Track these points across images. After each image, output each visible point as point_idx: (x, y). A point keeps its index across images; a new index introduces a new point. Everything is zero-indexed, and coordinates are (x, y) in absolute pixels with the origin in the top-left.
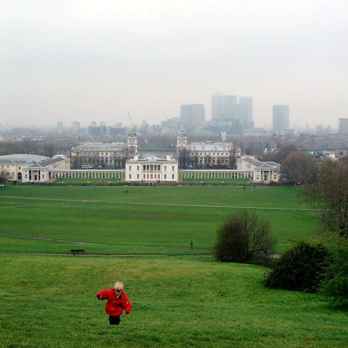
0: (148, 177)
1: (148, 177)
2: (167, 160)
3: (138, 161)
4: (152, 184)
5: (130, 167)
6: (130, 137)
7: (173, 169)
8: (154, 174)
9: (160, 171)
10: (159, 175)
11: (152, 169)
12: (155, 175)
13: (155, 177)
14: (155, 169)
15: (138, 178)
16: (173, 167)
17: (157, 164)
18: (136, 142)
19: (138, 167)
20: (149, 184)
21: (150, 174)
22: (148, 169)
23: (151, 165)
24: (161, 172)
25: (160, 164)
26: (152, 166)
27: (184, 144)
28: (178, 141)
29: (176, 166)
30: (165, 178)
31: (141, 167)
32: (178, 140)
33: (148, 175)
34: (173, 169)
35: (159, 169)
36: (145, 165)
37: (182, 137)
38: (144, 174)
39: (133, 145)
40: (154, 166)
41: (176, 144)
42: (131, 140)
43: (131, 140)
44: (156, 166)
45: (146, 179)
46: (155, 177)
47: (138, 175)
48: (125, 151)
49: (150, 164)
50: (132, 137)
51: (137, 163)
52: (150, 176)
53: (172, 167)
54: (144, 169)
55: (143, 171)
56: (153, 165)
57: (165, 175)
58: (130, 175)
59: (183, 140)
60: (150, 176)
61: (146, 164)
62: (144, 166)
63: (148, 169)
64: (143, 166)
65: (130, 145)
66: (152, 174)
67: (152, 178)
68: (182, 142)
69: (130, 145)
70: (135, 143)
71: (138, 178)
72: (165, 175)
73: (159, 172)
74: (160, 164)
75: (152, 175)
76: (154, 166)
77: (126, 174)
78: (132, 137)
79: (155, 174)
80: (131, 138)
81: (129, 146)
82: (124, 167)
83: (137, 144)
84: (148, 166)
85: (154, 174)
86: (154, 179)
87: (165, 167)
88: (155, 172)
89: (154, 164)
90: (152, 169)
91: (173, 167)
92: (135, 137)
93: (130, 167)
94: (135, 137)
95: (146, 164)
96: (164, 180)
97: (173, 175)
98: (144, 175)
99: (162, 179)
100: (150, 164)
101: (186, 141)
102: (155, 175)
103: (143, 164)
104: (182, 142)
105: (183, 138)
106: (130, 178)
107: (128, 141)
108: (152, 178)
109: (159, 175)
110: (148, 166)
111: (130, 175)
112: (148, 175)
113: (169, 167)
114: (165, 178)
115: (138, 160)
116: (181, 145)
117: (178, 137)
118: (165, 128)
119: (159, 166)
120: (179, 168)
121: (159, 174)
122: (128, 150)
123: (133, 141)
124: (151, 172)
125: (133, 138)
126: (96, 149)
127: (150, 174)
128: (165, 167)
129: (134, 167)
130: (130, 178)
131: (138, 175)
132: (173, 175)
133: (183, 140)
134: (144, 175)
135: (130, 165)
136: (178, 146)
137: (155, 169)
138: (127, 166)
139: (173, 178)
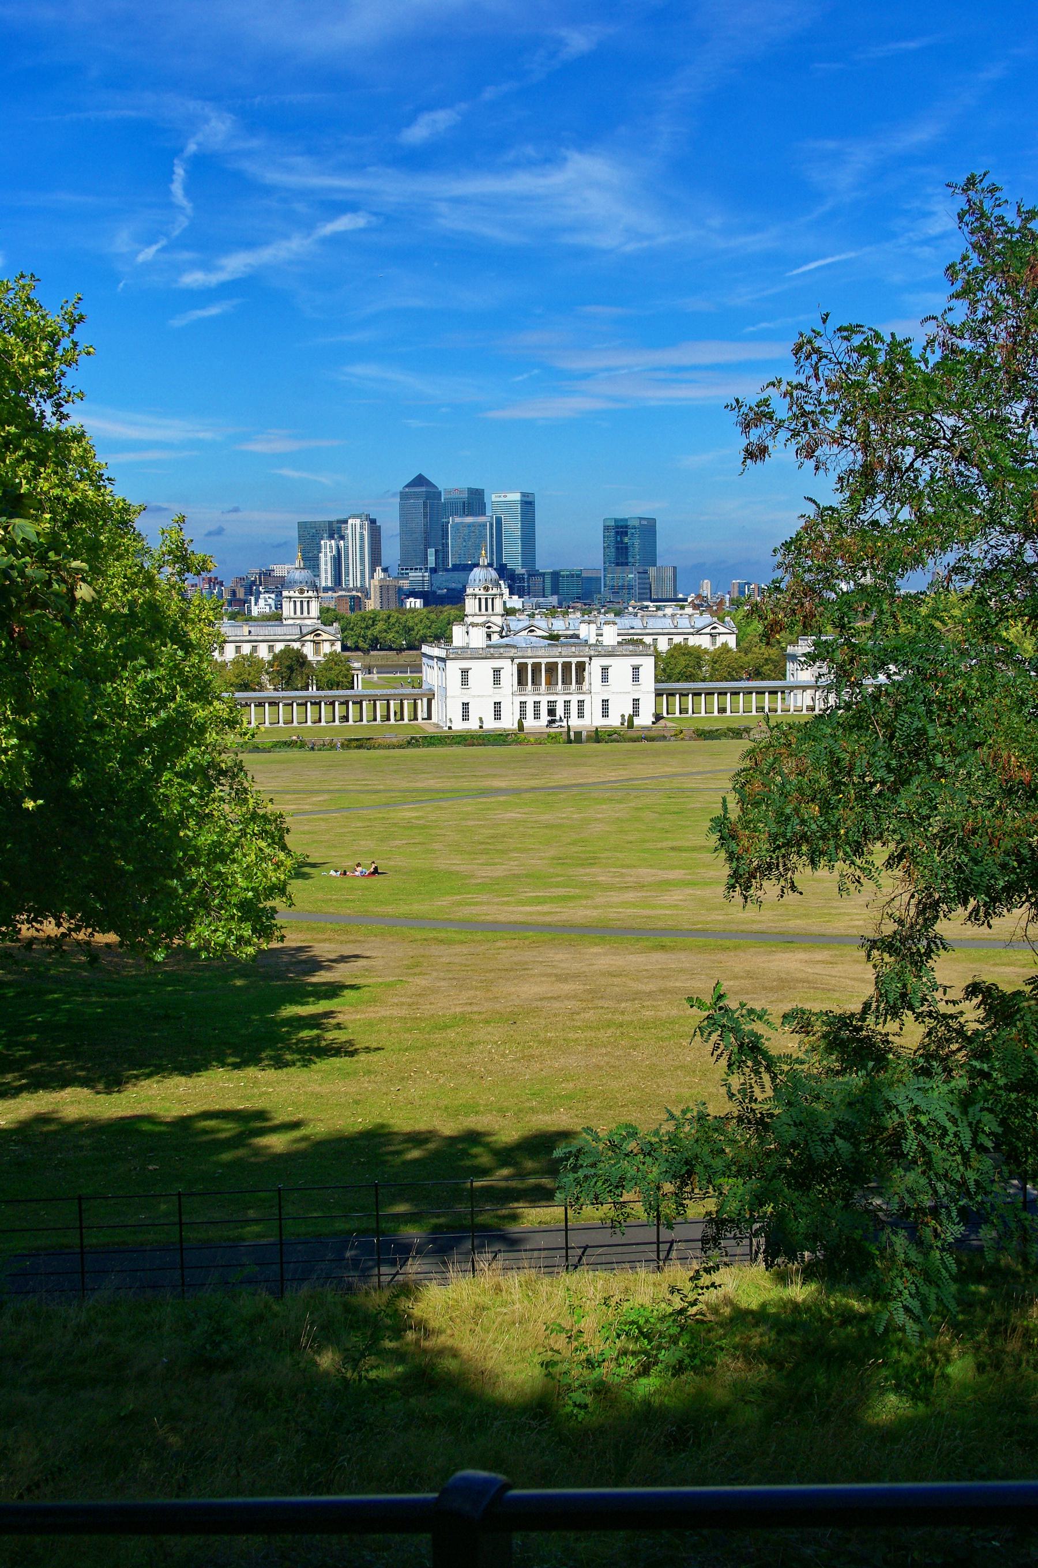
0: (537, 716)
1: (537, 716)
4: (584, 734)
5: (465, 672)
6: (292, 594)
7: (636, 678)
8: (560, 700)
9: (585, 686)
10: (581, 703)
11: (551, 682)
12: (567, 703)
15: (497, 716)
16: (636, 669)
17: (574, 660)
19: (497, 672)
23: (547, 664)
25: (587, 659)
26: (551, 668)
29: (648, 666)
30: (605, 714)
31: (509, 672)
33: (537, 704)
34: (636, 678)
37: (487, 589)
38: (523, 699)
42: (298, 604)
43: (298, 604)
44: (567, 666)
47: (497, 704)
48: (308, 638)
49: (544, 661)
50: (302, 592)
51: (492, 657)
54: (521, 681)
57: (605, 702)
58: (466, 705)
59: (490, 601)
62: (522, 669)
64: (515, 667)
66: (552, 698)
67: (552, 712)
68: (487, 610)
72: (605, 702)
73: (579, 691)
74: (587, 659)
78: (302, 592)
79: (567, 698)
80: (297, 594)
84: (536, 667)
85: (560, 700)
87: (605, 669)
89: (560, 661)
90: (549, 683)
91: (636, 669)
93: (465, 672)
94: (311, 594)
95: (530, 661)
96: (599, 721)
97: (636, 701)
98: (523, 704)
99: (593, 719)
102: (567, 703)
103: (517, 661)
104: (487, 610)
106: (465, 717)
109: (581, 703)
111: (466, 705)
112: (537, 704)
113: (621, 667)
115: (488, 647)
117: (469, 591)
118: (267, 595)
119: (581, 667)
121: (581, 697)
122: (319, 635)
123: (305, 604)
127: (544, 700)
128: (605, 669)
130: (465, 717)
131: (497, 704)
132: (636, 701)
133: (490, 601)
134: (523, 704)
135: (465, 664)
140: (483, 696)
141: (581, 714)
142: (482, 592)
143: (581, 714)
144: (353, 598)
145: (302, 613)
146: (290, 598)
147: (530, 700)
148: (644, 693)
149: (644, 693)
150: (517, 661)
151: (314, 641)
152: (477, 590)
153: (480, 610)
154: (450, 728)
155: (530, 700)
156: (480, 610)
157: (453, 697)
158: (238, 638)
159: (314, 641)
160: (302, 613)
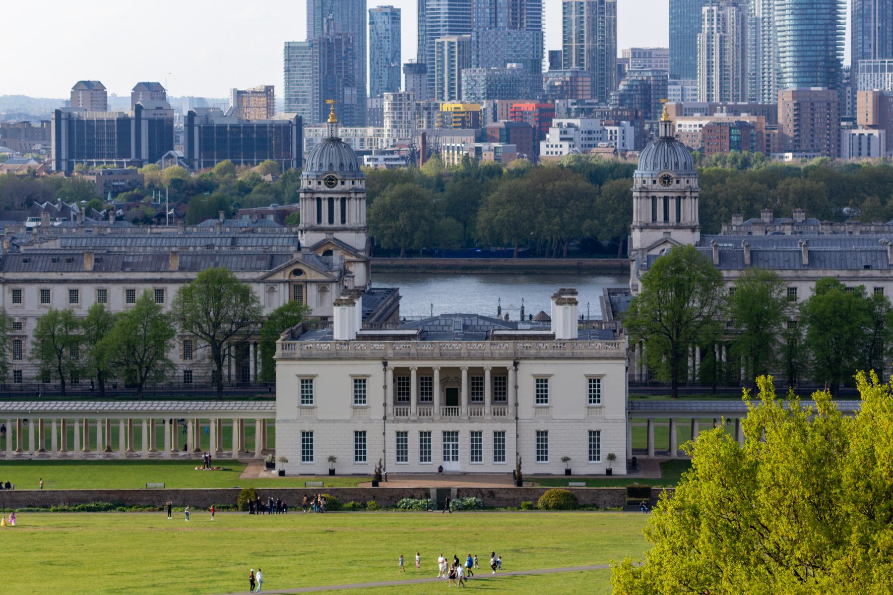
0: (425, 454)
1: (425, 454)
2: (552, 337)
3: (363, 345)
5: (307, 385)
6: (314, 185)
9: (510, 409)
10: (499, 437)
11: (452, 398)
12: (476, 436)
13: (476, 454)
14: (476, 395)
15: (360, 454)
16: (594, 384)
18: (357, 212)
19: (360, 383)
20: (433, 493)
21: (437, 429)
22: (426, 395)
23: (443, 370)
24: (517, 418)
25: (509, 364)
26: (450, 376)
27: (678, 227)
28: (640, 210)
30: (542, 453)
32: (635, 200)
33: (425, 437)
35: (500, 394)
36: (407, 370)
37: (666, 180)
38: (401, 427)
39: (338, 236)
40: (464, 374)
41: (626, 231)
42: (325, 205)
43: (325, 205)
45: (414, 463)
46: (476, 454)
47: (360, 437)
48: (280, 276)
50: (331, 182)
52: (437, 444)
53: (585, 384)
54: (402, 395)
55: (390, 409)
56: (458, 370)
57: (542, 435)
58: (307, 438)
59: (672, 204)
60: (437, 444)
61: (414, 365)
62: (401, 379)
63: (426, 395)
64: (390, 374)
65: (321, 236)
66: (450, 427)
67: (451, 453)
68: (666, 218)
69: (321, 236)
70: (347, 225)
71: (360, 454)
72: (542, 435)
74: (509, 364)
75: (450, 436)
76: (464, 374)
77: (278, 427)
80: (323, 187)
81: (307, 240)
82: (266, 389)
83: (365, 229)
86: (462, 464)
88: (475, 415)
89: (465, 365)
90: (452, 398)
92: (348, 185)
93: (307, 385)
94: (348, 185)
95: (414, 365)
97: (594, 436)
98: (402, 436)
100: (436, 365)
101: (690, 211)
102: (476, 436)
103: (392, 364)
104: (666, 218)
105: (674, 185)
106: (307, 453)
107: (306, 211)
108: (451, 453)
109: (499, 437)
110: (425, 378)
112: (425, 437)
113: (568, 380)
114: (542, 453)
115: (360, 338)
116: (659, 235)
117: (638, 183)
118: (565, 122)
120: (639, 389)
122: (298, 272)
123: (337, 205)
124: (441, 420)
125: (339, 187)
126: (89, 264)
127: (437, 429)
129: (333, 380)
130: (307, 453)
131: (360, 437)
132: (594, 436)
133: (672, 204)
134: (402, 436)
135: (307, 368)
136: (637, 239)
137: (476, 395)
138: (287, 375)
139: (594, 453)
140: (335, 421)
141: (499, 455)
142: (658, 186)
143: (499, 455)
144: (742, 125)
145: (331, 220)
146: (312, 192)
147: (414, 432)
148: (606, 421)
149: (606, 421)
150: (392, 364)
151: (289, 282)
152: (649, 182)
153: (654, 219)
154: (282, 473)
155: (414, 432)
156: (654, 219)
157: (285, 421)
158: (157, 276)
159: (289, 282)
160: (331, 220)
